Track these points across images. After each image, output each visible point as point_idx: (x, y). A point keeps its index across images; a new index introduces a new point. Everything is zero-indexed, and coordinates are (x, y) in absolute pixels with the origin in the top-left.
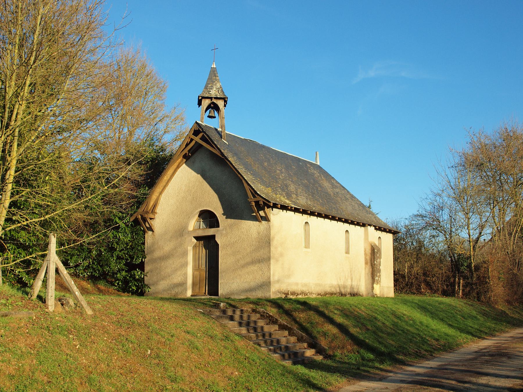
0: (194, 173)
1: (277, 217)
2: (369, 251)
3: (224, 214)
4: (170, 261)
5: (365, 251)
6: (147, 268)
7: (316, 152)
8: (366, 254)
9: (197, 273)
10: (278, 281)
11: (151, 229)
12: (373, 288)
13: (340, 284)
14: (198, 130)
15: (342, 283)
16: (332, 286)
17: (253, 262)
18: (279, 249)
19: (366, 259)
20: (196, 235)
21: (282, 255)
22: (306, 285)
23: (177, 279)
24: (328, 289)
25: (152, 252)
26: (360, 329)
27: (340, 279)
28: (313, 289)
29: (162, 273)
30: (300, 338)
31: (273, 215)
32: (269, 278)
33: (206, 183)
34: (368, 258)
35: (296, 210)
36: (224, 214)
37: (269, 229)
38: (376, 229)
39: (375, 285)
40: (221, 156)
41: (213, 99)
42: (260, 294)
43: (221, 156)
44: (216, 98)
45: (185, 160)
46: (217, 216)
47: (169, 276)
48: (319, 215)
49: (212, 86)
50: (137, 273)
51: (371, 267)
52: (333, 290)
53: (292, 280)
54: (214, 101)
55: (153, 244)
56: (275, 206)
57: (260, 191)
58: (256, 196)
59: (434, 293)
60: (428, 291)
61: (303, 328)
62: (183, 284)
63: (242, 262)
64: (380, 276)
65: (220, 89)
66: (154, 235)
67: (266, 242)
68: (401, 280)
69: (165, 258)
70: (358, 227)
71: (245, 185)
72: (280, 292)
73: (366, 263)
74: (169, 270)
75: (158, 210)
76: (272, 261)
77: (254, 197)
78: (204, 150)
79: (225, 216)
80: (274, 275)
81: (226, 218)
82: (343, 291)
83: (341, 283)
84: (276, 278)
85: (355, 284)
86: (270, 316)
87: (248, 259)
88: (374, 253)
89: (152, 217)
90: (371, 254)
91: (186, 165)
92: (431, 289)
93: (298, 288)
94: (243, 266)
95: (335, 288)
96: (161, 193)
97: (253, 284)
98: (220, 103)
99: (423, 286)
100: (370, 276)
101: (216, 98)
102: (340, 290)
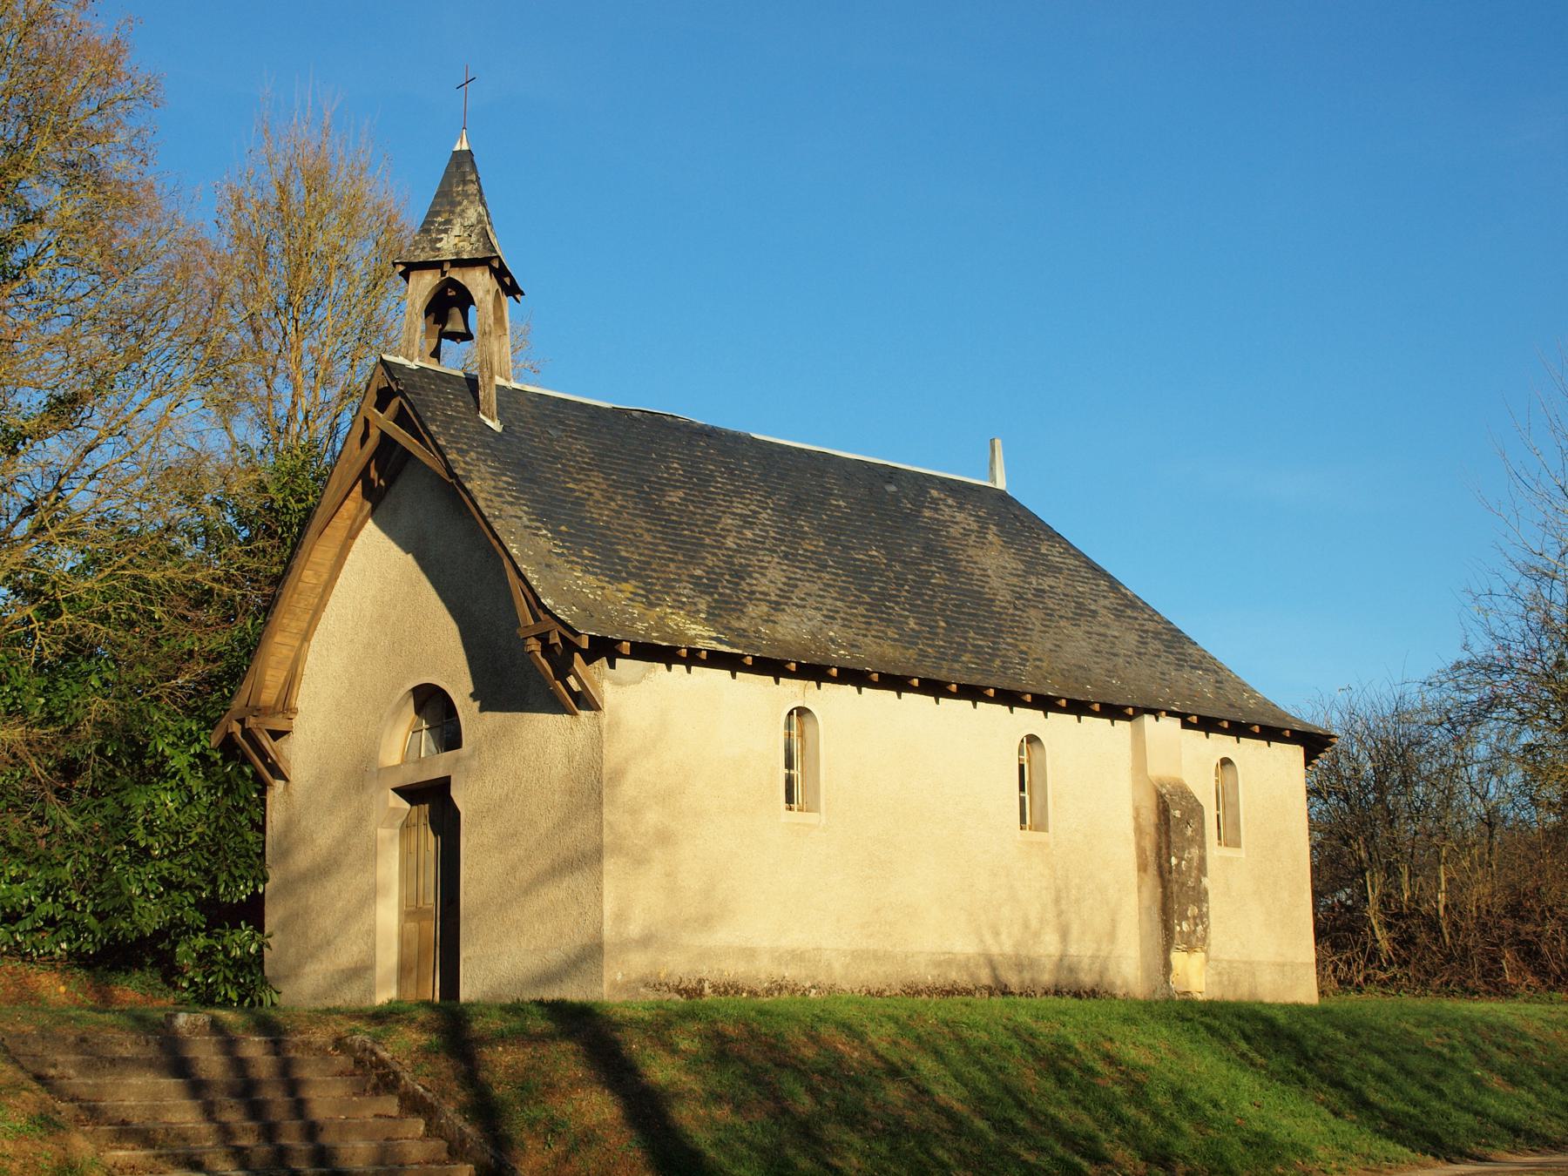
0: (396, 551)
1: (634, 695)
2: (1150, 817)
3: (474, 696)
4: (332, 886)
5: (1136, 818)
6: (272, 919)
7: (992, 441)
8: (1139, 830)
9: (412, 926)
10: (646, 941)
11: (278, 773)
12: (1167, 966)
13: (994, 950)
14: (392, 389)
15: (1008, 948)
16: (949, 963)
17: (554, 869)
18: (652, 817)
19: (1141, 852)
20: (399, 783)
21: (664, 838)
22: (797, 956)
23: (346, 955)
24: (928, 975)
25: (284, 854)
26: (738, 1108)
27: (997, 934)
28: (838, 969)
29: (311, 933)
30: (456, 1144)
31: (618, 683)
32: (599, 930)
33: (429, 585)
34: (1149, 845)
35: (731, 663)
36: (474, 696)
37: (597, 742)
38: (1186, 725)
39: (1177, 958)
40: (445, 475)
41: (447, 267)
42: (572, 992)
43: (445, 475)
44: (459, 263)
45: (368, 505)
46: (456, 703)
47: (329, 943)
48: (855, 677)
49: (448, 222)
50: (240, 940)
51: (1157, 881)
52: (955, 976)
53: (722, 937)
54: (456, 274)
55: (290, 824)
56: (605, 649)
57: (560, 595)
58: (541, 613)
59: (1550, 988)
60: (1530, 978)
61: (485, 1110)
62: (361, 971)
63: (525, 874)
64: (1202, 918)
65: (478, 229)
66: (290, 795)
67: (591, 788)
68: (1423, 938)
69: (324, 870)
70: (1096, 726)
71: (511, 575)
72: (656, 987)
73: (1142, 868)
74: (327, 922)
75: (303, 699)
76: (609, 865)
77: (536, 618)
78: (409, 465)
79: (478, 704)
80: (621, 917)
81: (482, 709)
82: (1012, 979)
83: (1004, 945)
84: (634, 930)
85: (1082, 950)
86: (382, 1063)
87: (542, 863)
88: (1171, 825)
89: (279, 724)
90: (1158, 828)
91: (375, 522)
92: (1542, 972)
93: (732, 969)
94: (530, 888)
95: (965, 966)
96: (306, 637)
97: (554, 956)
98: (480, 283)
99: (1508, 958)
100: (1156, 916)
101: (459, 263)
102: (996, 978)
